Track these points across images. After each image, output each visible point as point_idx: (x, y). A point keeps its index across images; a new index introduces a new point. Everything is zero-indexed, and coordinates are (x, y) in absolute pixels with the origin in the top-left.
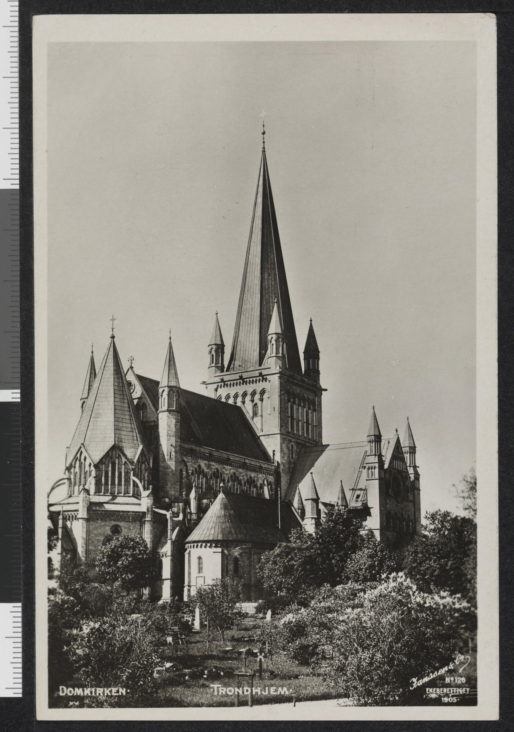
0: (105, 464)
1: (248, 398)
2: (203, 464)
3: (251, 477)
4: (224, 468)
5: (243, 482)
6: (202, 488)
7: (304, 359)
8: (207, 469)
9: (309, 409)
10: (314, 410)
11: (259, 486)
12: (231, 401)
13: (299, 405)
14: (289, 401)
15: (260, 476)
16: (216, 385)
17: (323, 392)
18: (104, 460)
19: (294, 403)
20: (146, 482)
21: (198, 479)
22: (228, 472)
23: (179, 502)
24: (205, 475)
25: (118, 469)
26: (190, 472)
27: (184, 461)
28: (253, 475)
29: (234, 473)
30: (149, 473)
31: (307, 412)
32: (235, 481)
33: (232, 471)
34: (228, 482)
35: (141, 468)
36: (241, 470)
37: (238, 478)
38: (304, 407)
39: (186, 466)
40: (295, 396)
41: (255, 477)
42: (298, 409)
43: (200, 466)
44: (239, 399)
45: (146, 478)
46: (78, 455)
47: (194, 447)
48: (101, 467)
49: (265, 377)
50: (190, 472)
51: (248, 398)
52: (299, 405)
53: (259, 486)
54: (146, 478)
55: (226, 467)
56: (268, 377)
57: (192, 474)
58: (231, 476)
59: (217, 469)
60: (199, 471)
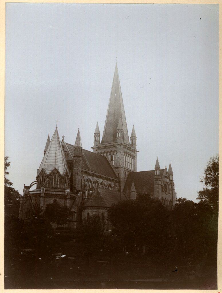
0: (52, 176)
1: (109, 154)
2: (91, 178)
3: (109, 183)
4: (99, 180)
5: (106, 185)
6: (89, 187)
7: (131, 140)
8: (92, 179)
9: (132, 158)
10: (134, 159)
11: (112, 187)
12: (102, 155)
13: (128, 157)
14: (124, 155)
15: (113, 183)
16: (97, 149)
17: (138, 152)
18: (51, 174)
19: (126, 156)
20: (68, 184)
21: (88, 183)
22: (100, 181)
23: (80, 192)
24: (91, 182)
25: (57, 178)
26: (85, 180)
27: (83, 176)
28: (110, 183)
29: (103, 182)
30: (69, 180)
31: (131, 160)
32: (103, 185)
33: (102, 181)
34: (100, 185)
35: (66, 178)
36: (105, 181)
37: (104, 184)
38: (130, 157)
39: (84, 178)
40: (126, 153)
41: (111, 183)
42: (128, 158)
43: (89, 178)
44: (105, 154)
45: (68, 182)
46: (42, 172)
47: (87, 171)
48: (50, 177)
49: (115, 146)
50: (85, 180)
51: (109, 154)
52: (128, 157)
53: (112, 187)
54: (68, 182)
55: (100, 179)
56: (116, 146)
57: (86, 181)
58: (102, 183)
59: (96, 180)
60: (89, 180)
